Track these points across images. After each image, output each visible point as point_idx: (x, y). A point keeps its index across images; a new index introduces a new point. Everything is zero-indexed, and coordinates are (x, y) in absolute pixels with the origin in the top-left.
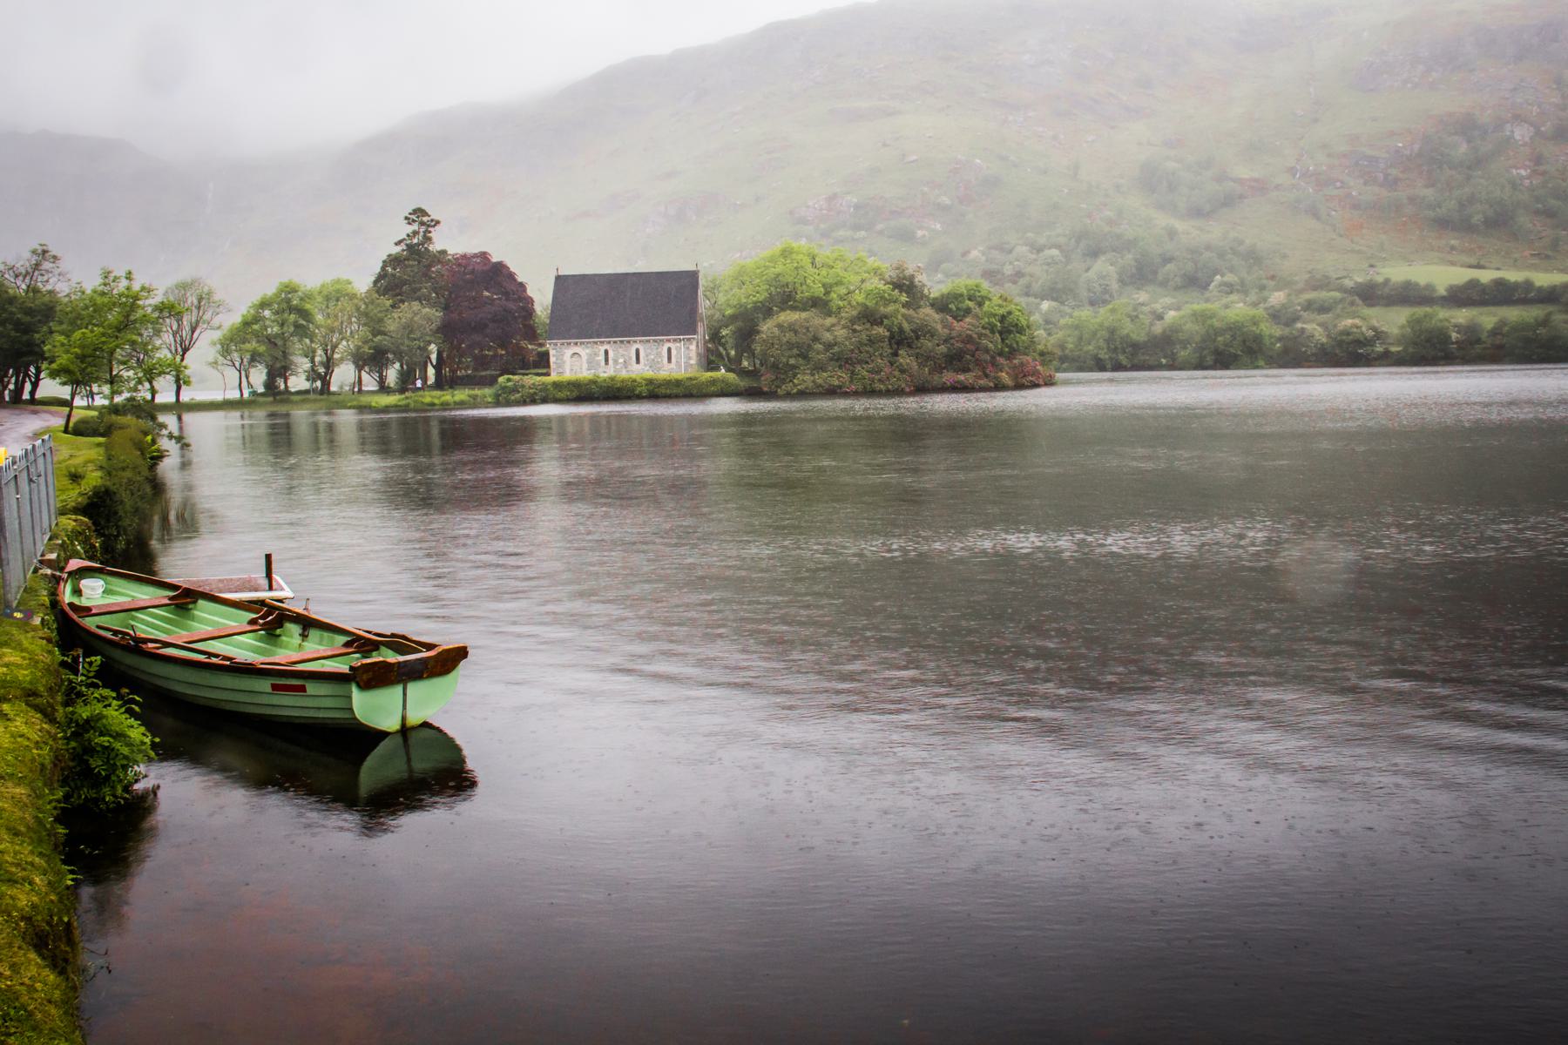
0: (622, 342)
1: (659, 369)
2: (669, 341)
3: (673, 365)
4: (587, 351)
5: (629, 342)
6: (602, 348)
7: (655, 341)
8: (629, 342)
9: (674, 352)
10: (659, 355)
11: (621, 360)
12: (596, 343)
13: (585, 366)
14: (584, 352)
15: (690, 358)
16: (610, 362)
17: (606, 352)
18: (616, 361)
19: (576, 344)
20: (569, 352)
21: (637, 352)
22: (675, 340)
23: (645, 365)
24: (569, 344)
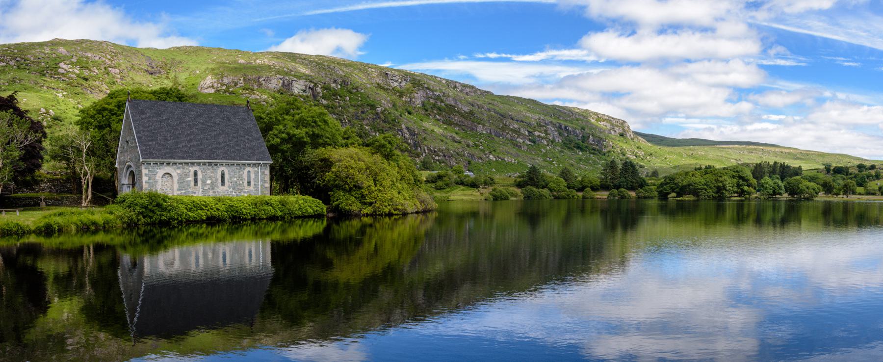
0: (210, 164)
1: (241, 190)
2: (249, 165)
3: (252, 188)
4: (179, 172)
5: (216, 164)
6: (192, 169)
7: (238, 165)
8: (216, 164)
10: (241, 178)
11: (209, 182)
12: (187, 164)
13: (176, 186)
14: (175, 172)
15: (265, 182)
16: (199, 183)
17: (195, 174)
18: (204, 182)
19: (168, 164)
20: (161, 172)
22: (254, 165)
23: (229, 187)
24: (162, 163)
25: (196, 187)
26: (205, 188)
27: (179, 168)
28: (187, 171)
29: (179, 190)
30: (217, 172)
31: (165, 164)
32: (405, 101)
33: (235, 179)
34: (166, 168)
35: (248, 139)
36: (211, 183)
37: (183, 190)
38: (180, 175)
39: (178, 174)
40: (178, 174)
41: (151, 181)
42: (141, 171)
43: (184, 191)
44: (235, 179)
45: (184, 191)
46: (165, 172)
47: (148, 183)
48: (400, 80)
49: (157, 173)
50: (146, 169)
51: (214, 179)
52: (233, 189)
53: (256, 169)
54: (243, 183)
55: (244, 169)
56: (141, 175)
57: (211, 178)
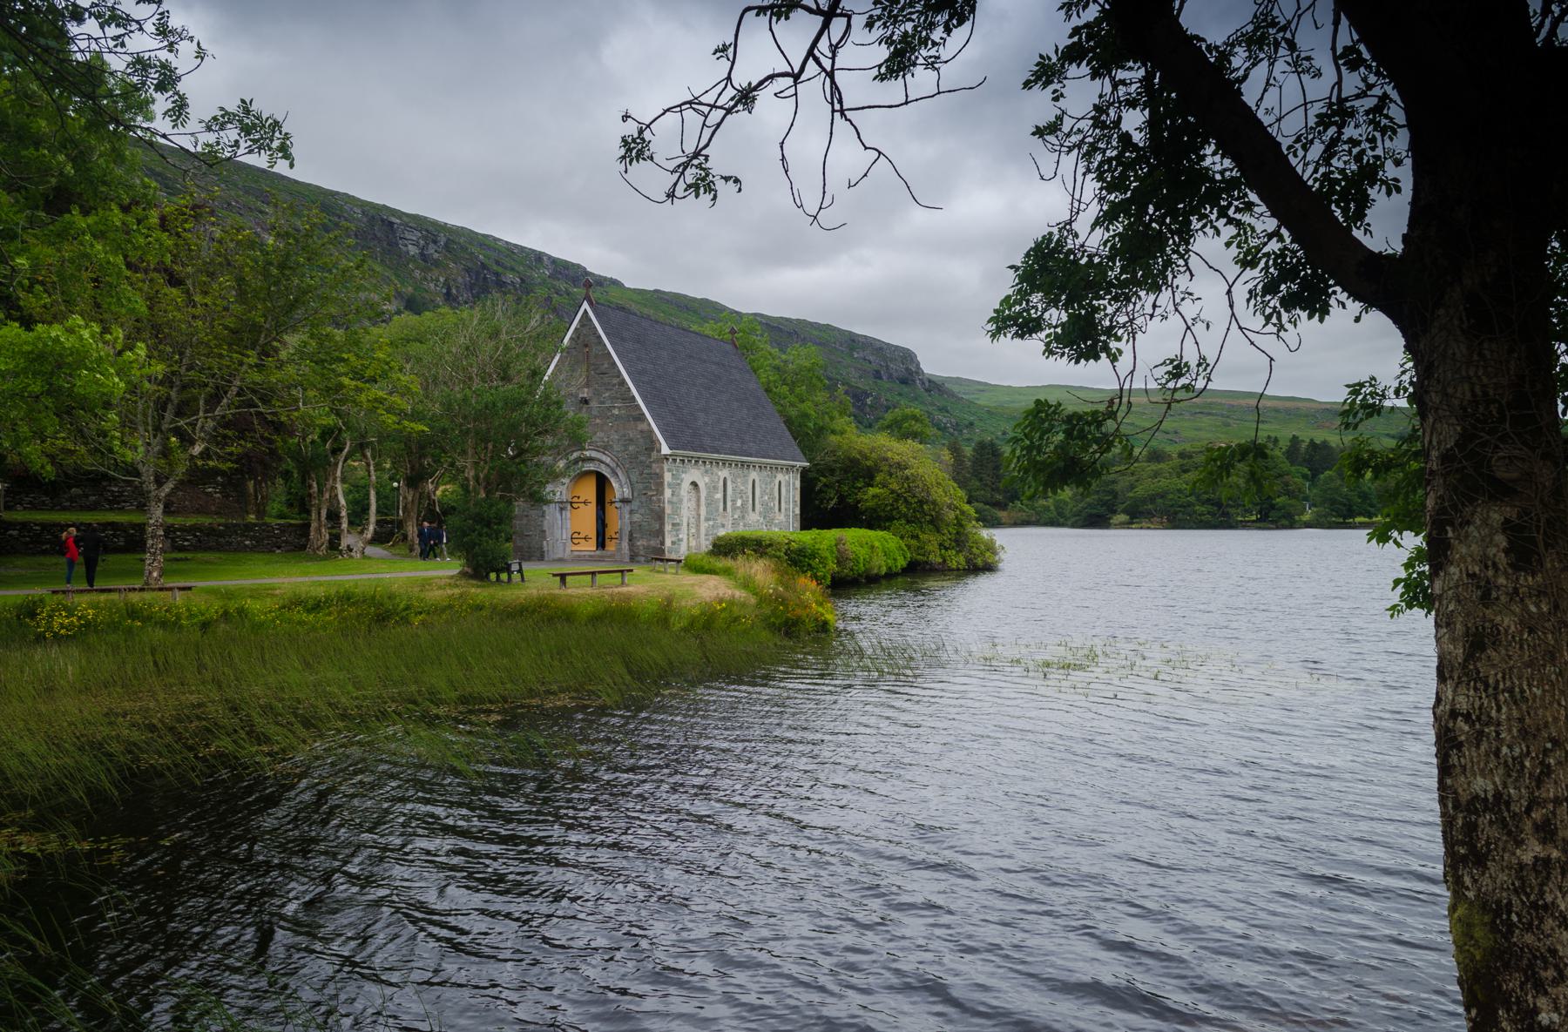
4: (707, 479)
10: (771, 494)
11: (739, 503)
16: (729, 504)
18: (734, 501)
27: (706, 472)
29: (707, 519)
41: (675, 499)
42: (660, 476)
48: (422, 242)
50: (669, 470)
56: (662, 484)
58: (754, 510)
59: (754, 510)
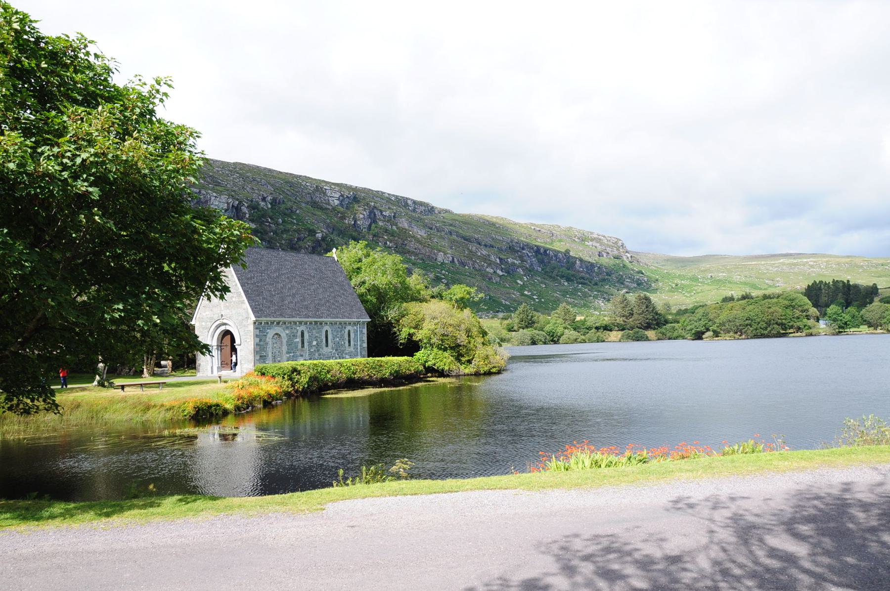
4: (287, 332)
6: (300, 329)
9: (352, 335)
10: (342, 337)
11: (315, 343)
13: (285, 348)
16: (306, 344)
18: (310, 343)
21: (327, 331)
22: (355, 324)
23: (333, 348)
25: (303, 349)
26: (312, 350)
27: (287, 328)
28: (295, 331)
29: (288, 353)
30: (321, 332)
31: (275, 323)
32: (349, 223)
33: (338, 339)
34: (276, 328)
35: (344, 294)
36: (317, 344)
37: (291, 353)
38: (290, 336)
39: (287, 334)
40: (287, 334)
41: (262, 343)
43: (292, 354)
44: (338, 339)
45: (292, 354)
46: (275, 333)
47: (259, 345)
49: (267, 333)
51: (319, 340)
52: (336, 350)
53: (355, 328)
54: (345, 343)
55: (345, 328)
57: (316, 338)
58: (327, 346)
59: (327, 346)
